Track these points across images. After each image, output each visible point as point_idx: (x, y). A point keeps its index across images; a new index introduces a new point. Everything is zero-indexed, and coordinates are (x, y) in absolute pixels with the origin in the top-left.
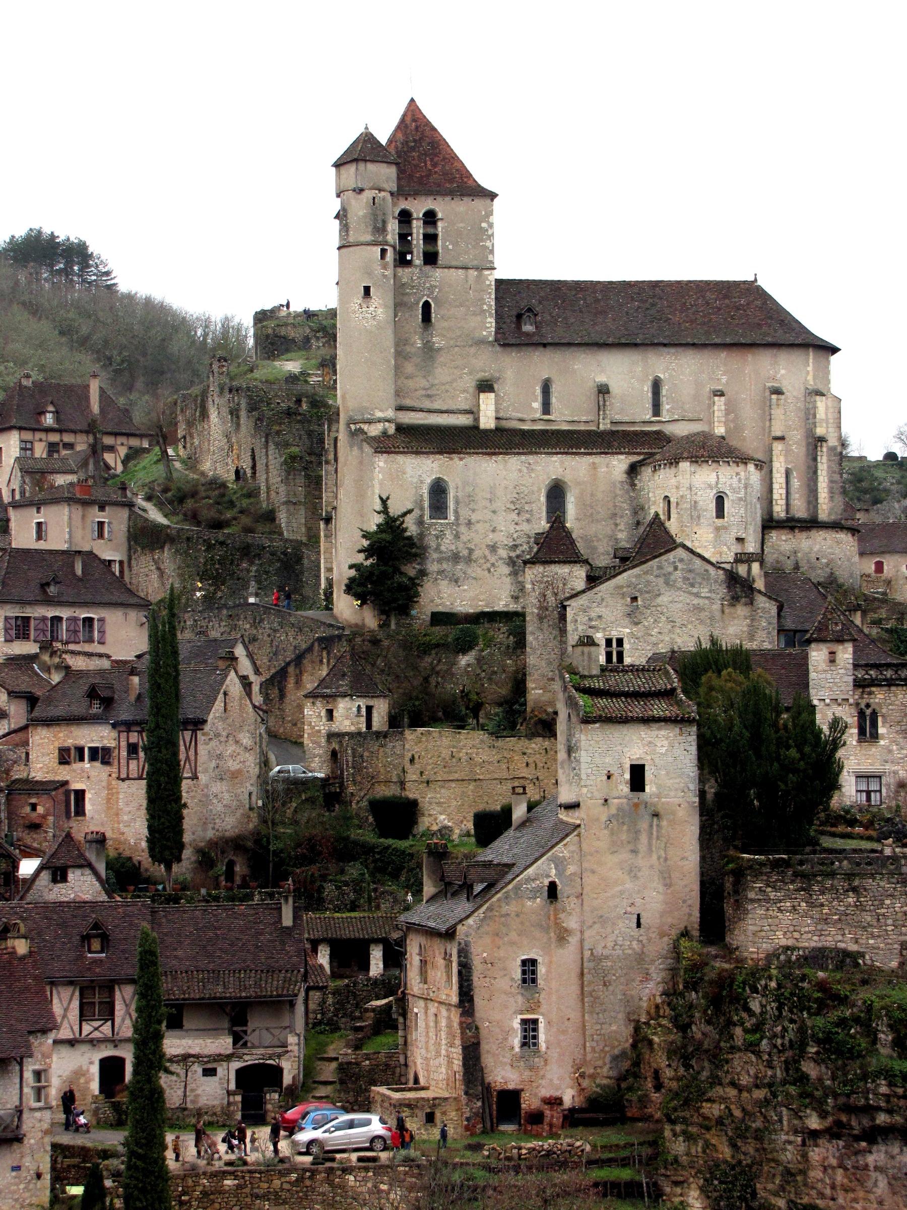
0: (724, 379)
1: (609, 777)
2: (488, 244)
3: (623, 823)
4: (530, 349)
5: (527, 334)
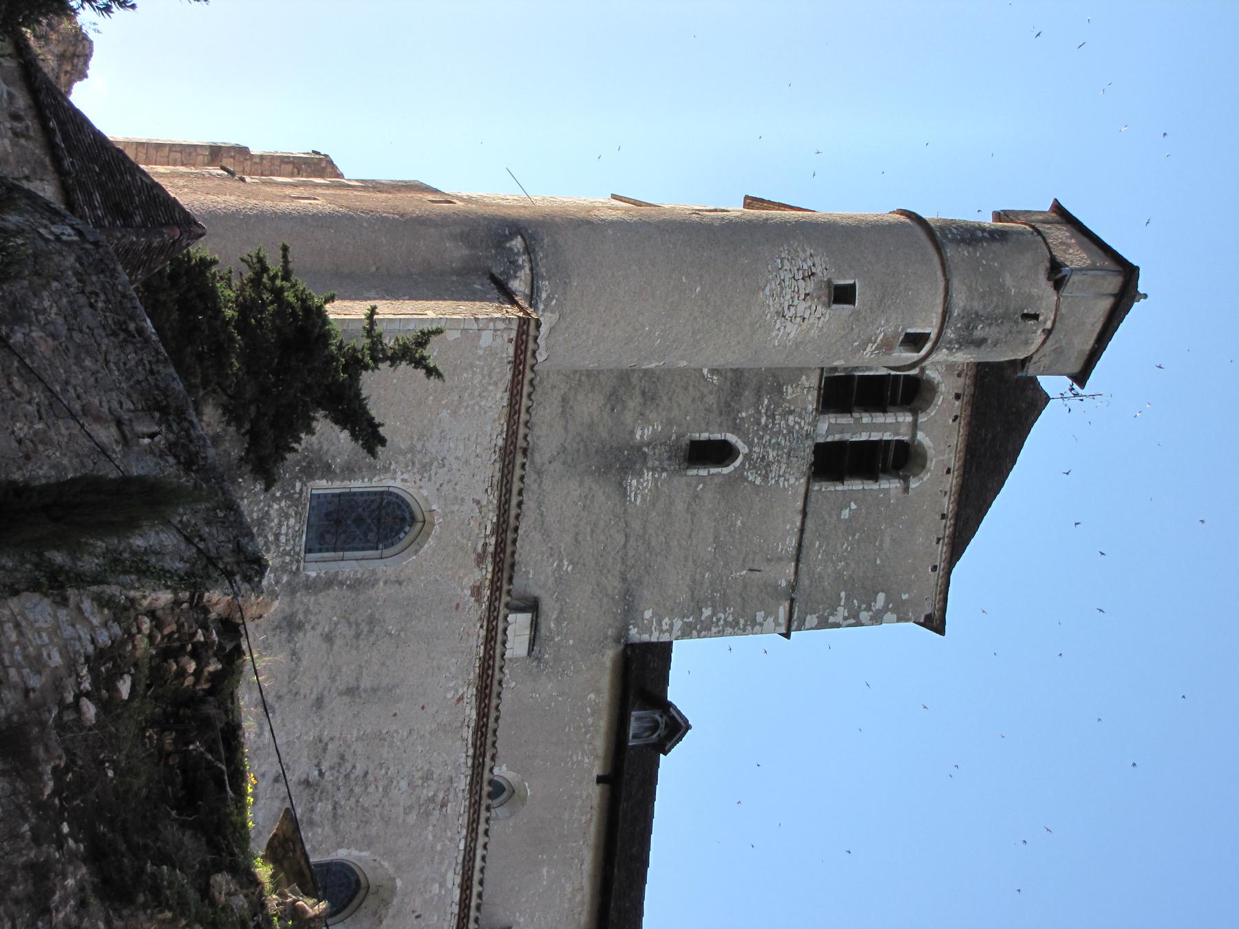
2: (842, 611)
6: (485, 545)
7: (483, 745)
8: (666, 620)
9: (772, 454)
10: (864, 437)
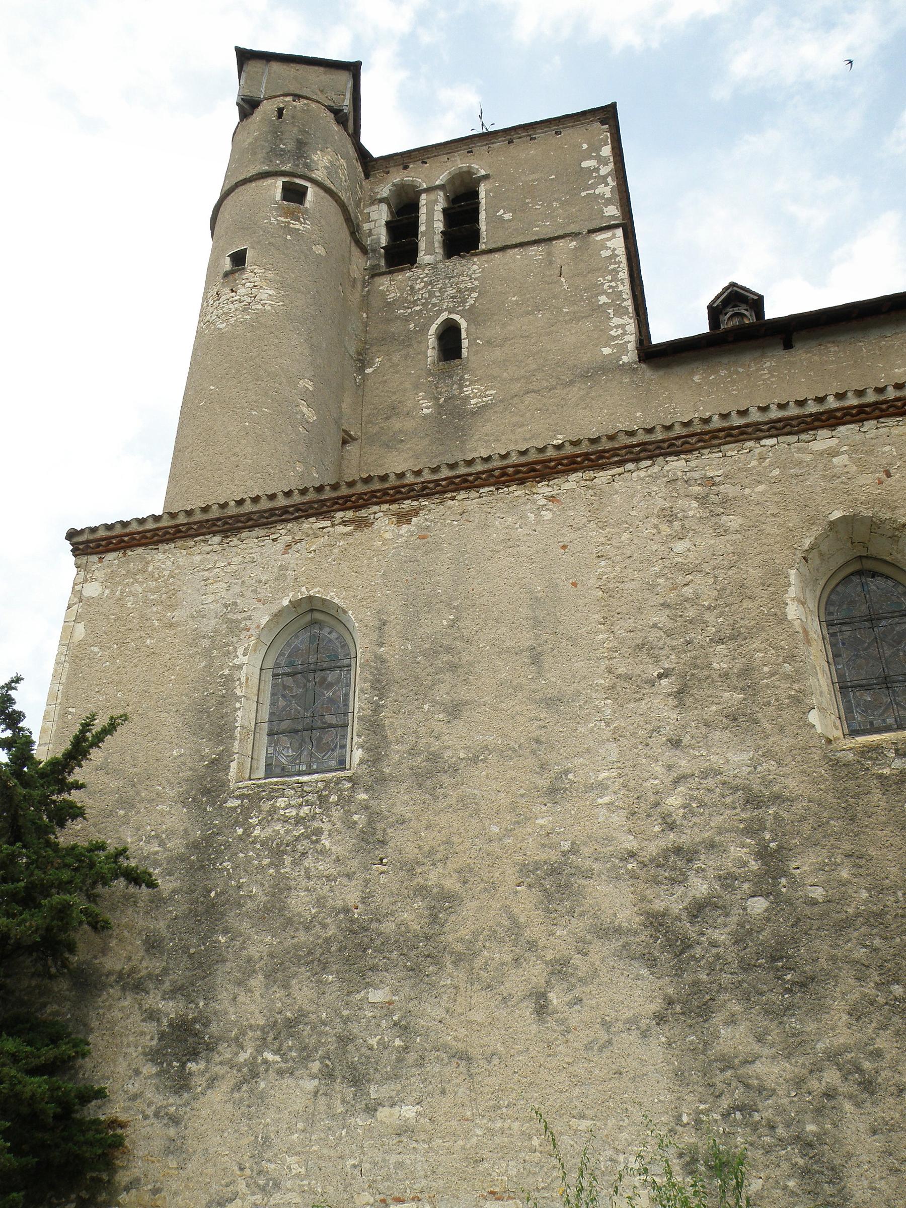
6: (344, 523)
7: (615, 451)
8: (613, 333)
9: (451, 291)
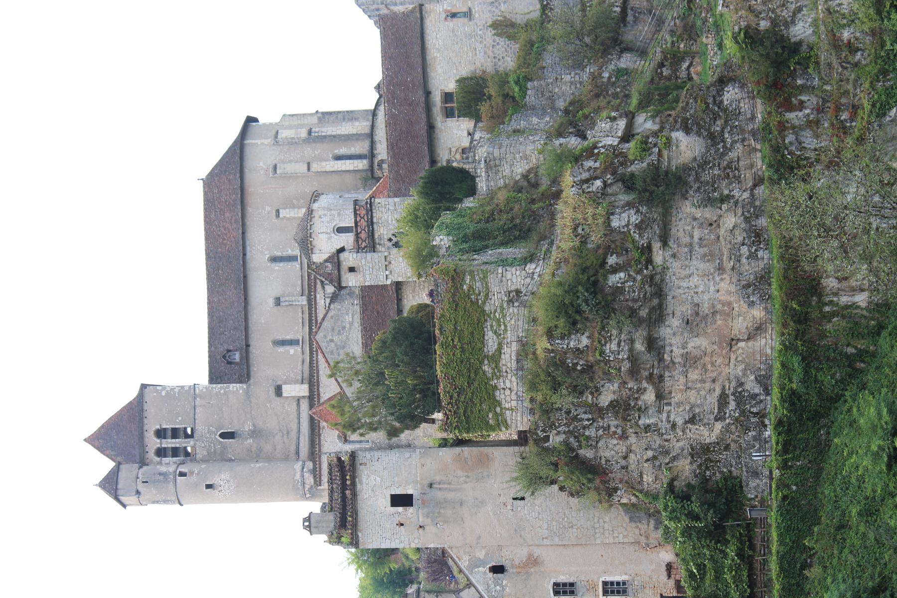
0: (268, 208)
1: (402, 525)
2: (177, 390)
3: (439, 513)
4: (251, 356)
5: (241, 359)
10: (177, 440)
